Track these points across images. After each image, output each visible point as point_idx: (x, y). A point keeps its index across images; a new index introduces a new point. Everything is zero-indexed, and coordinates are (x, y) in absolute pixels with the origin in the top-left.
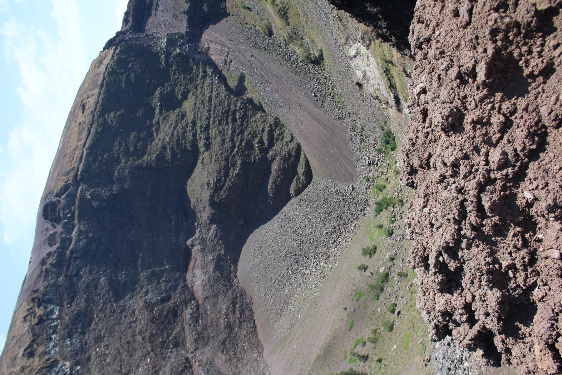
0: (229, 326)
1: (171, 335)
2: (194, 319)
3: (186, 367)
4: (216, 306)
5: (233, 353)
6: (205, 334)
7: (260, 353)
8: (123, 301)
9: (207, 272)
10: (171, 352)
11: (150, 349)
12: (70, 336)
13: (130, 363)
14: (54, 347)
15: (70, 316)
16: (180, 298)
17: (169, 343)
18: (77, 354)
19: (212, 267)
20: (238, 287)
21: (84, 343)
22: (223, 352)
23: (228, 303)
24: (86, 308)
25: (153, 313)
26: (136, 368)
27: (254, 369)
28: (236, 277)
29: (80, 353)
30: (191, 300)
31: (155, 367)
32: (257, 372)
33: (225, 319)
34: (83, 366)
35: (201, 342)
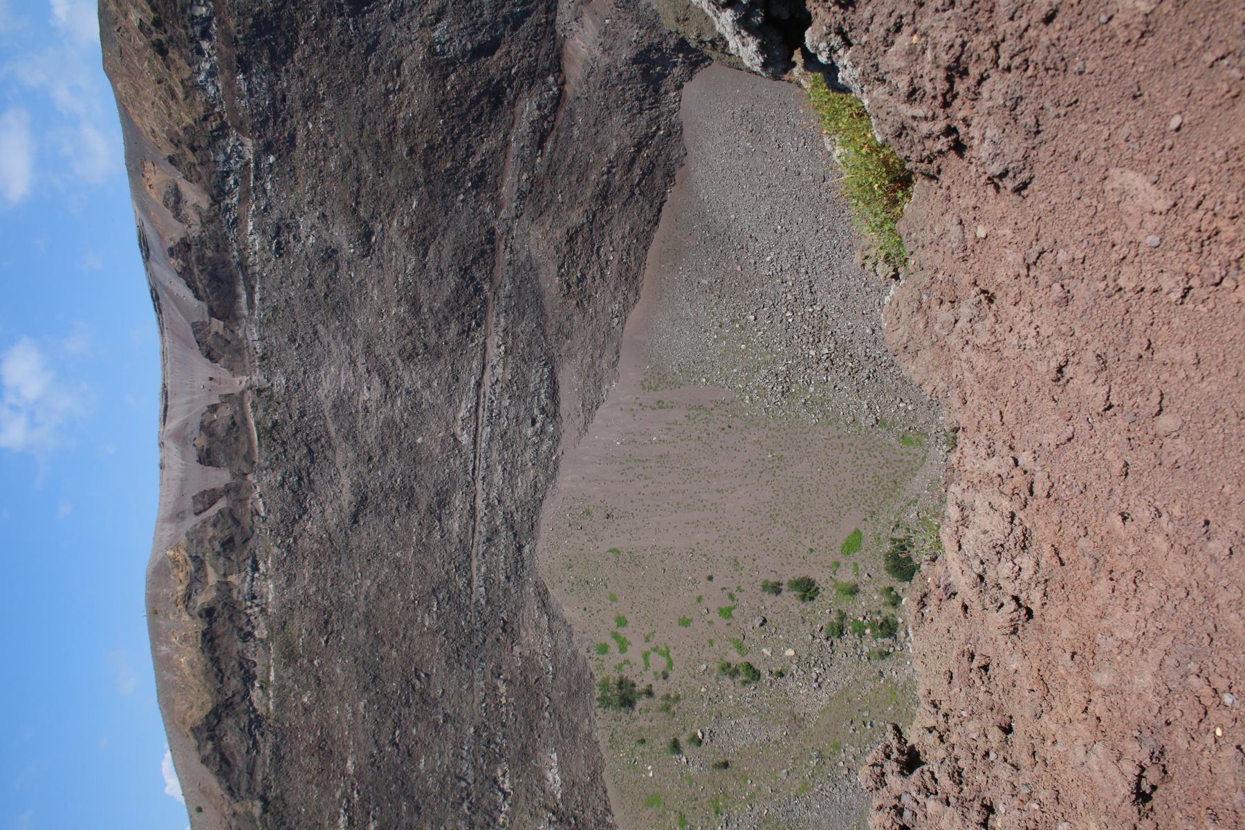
0: (604, 196)
1: (474, 153)
2: (538, 134)
3: (483, 252)
4: (599, 127)
5: (579, 275)
6: (547, 190)
7: (627, 307)
8: (375, 13)
9: (611, 48)
10: (463, 201)
11: (422, 180)
12: (244, 66)
13: (376, 192)
14: (211, 74)
15: (238, 26)
16: (523, 57)
17: (465, 174)
18: (264, 123)
19: (626, 54)
20: (673, 112)
21: (279, 97)
22: (560, 268)
23: (628, 141)
24: (276, 10)
25: (445, 86)
26: (388, 215)
27: (595, 348)
28: (679, 87)
29: (272, 121)
30: (548, 71)
31: (425, 228)
32: (594, 363)
33: (603, 175)
34: (280, 156)
35: (531, 204)
